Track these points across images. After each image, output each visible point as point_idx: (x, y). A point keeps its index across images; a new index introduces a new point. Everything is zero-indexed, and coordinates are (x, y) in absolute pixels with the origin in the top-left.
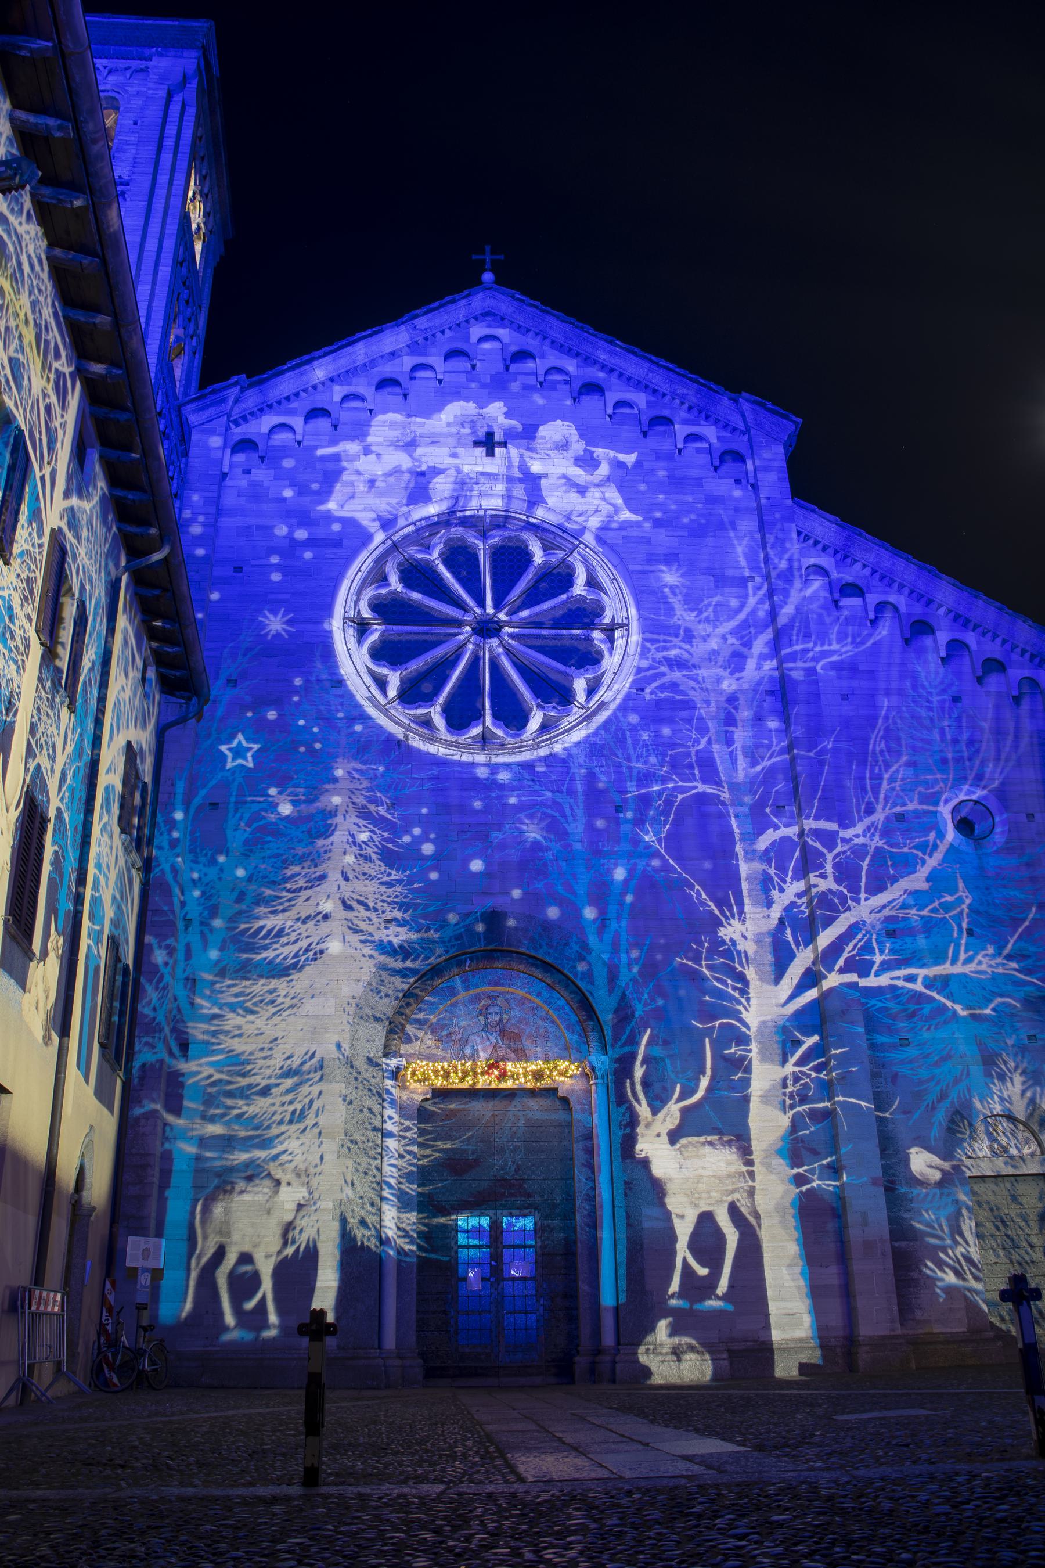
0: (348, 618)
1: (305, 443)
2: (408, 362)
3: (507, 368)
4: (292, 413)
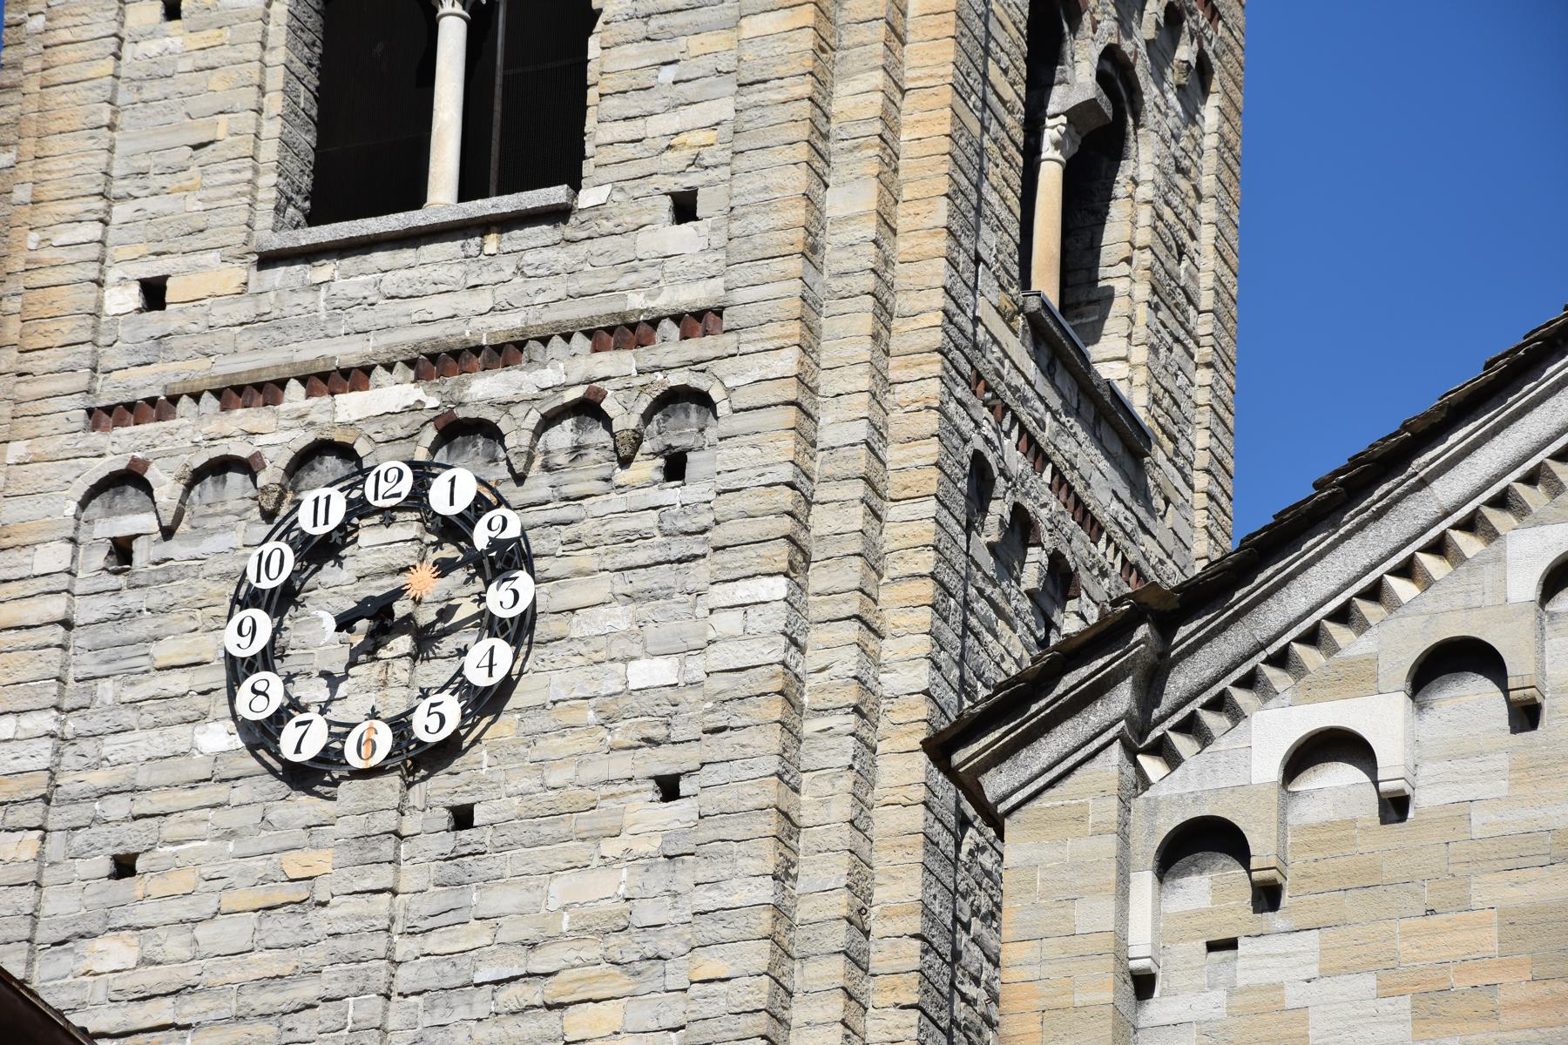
4: (1362, 679)
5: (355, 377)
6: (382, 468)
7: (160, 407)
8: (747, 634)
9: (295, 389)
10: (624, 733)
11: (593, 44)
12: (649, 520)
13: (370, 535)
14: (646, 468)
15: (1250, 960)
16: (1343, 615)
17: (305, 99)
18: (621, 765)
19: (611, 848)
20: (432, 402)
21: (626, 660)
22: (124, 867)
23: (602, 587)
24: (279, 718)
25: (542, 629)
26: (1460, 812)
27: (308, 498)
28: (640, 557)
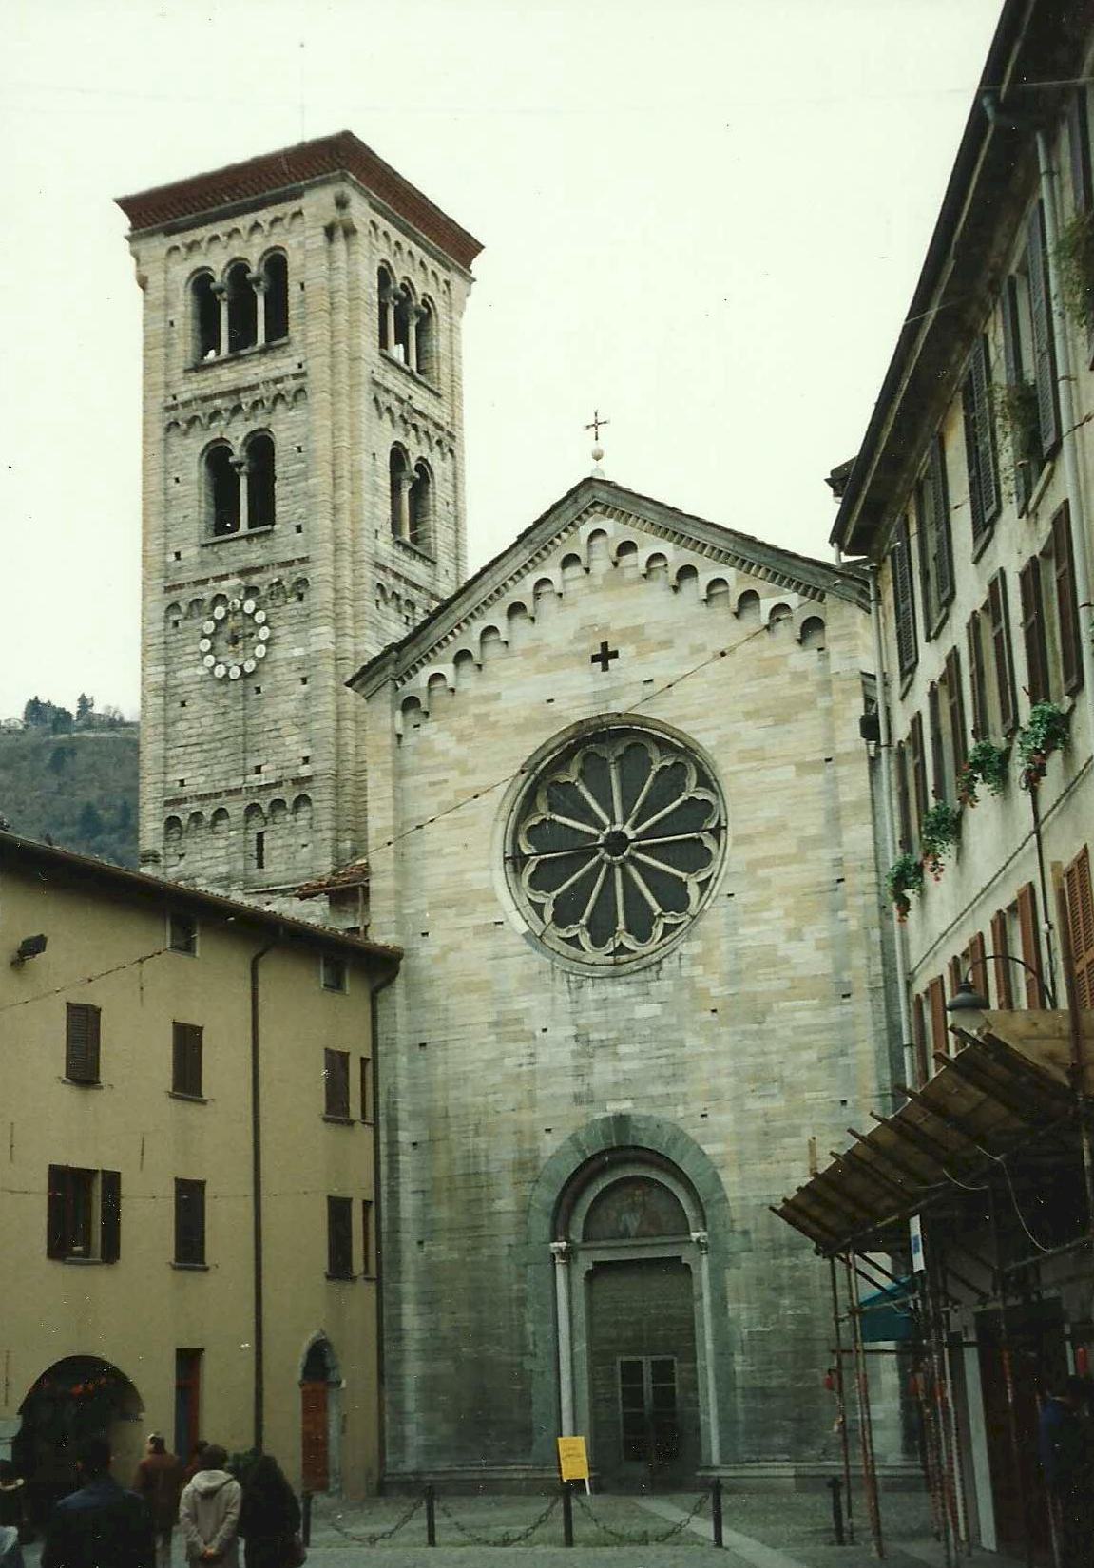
0: (509, 858)
1: (458, 689)
2: (531, 579)
3: (615, 564)
4: (443, 661)
5: (225, 577)
7: (181, 586)
9: (211, 581)
10: (293, 667)
11: (276, 485)
12: (295, 612)
16: (439, 645)
17: (211, 500)
19: (292, 697)
20: (243, 583)
22: (183, 704)
24: (213, 667)
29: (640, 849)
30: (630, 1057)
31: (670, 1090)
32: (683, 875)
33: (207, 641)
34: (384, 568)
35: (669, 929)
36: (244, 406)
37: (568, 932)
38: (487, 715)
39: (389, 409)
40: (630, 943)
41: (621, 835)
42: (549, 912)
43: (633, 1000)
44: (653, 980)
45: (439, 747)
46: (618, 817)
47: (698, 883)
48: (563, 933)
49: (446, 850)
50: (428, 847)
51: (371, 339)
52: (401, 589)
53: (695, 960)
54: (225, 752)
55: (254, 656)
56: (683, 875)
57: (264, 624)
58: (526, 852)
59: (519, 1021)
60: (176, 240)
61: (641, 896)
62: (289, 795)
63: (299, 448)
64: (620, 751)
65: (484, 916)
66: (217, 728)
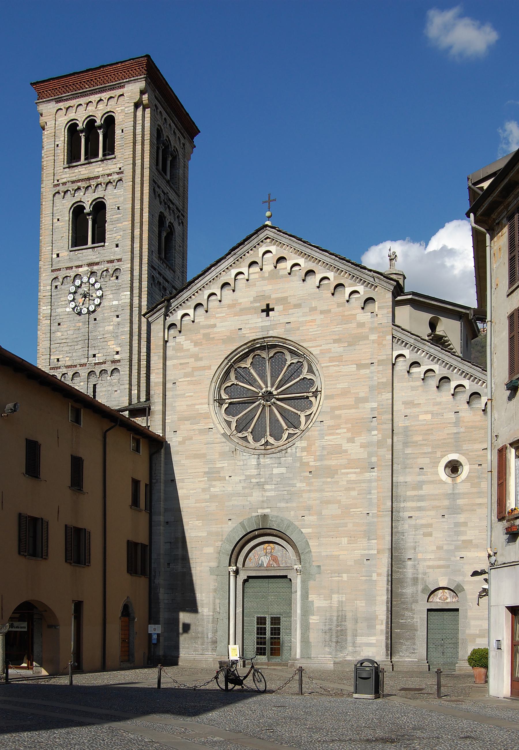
0: (215, 400)
5: (81, 266)
6: (84, 278)
8: (125, 299)
10: (113, 310)
11: (106, 224)
13: (83, 285)
14: (114, 278)
15: (178, 339)
18: (112, 314)
19: (112, 323)
21: (113, 301)
23: (109, 292)
25: (104, 297)
26: (199, 322)
27: (76, 281)
28: (114, 289)
29: (278, 399)
30: (271, 490)
31: (289, 505)
32: (299, 413)
33: (71, 295)
34: (155, 269)
35: (290, 435)
36: (92, 186)
37: (242, 434)
38: (209, 334)
39: (159, 195)
40: (271, 440)
41: (271, 393)
42: (234, 425)
43: (273, 465)
44: (283, 457)
45: (185, 347)
46: (269, 385)
47: (305, 416)
48: (240, 435)
49: (186, 394)
50: (179, 393)
51: (153, 161)
52: (161, 280)
53: (303, 449)
54: (79, 347)
55: (94, 304)
56: (299, 413)
57: (99, 289)
58: (224, 397)
59: (219, 472)
60: (61, 105)
61: (278, 420)
62: (109, 367)
63: (118, 208)
64: (271, 355)
65: (202, 426)
66: (75, 336)
